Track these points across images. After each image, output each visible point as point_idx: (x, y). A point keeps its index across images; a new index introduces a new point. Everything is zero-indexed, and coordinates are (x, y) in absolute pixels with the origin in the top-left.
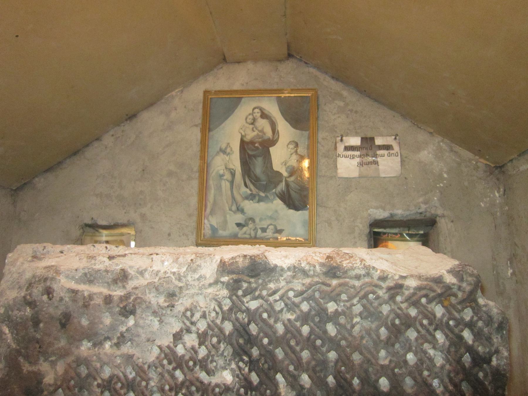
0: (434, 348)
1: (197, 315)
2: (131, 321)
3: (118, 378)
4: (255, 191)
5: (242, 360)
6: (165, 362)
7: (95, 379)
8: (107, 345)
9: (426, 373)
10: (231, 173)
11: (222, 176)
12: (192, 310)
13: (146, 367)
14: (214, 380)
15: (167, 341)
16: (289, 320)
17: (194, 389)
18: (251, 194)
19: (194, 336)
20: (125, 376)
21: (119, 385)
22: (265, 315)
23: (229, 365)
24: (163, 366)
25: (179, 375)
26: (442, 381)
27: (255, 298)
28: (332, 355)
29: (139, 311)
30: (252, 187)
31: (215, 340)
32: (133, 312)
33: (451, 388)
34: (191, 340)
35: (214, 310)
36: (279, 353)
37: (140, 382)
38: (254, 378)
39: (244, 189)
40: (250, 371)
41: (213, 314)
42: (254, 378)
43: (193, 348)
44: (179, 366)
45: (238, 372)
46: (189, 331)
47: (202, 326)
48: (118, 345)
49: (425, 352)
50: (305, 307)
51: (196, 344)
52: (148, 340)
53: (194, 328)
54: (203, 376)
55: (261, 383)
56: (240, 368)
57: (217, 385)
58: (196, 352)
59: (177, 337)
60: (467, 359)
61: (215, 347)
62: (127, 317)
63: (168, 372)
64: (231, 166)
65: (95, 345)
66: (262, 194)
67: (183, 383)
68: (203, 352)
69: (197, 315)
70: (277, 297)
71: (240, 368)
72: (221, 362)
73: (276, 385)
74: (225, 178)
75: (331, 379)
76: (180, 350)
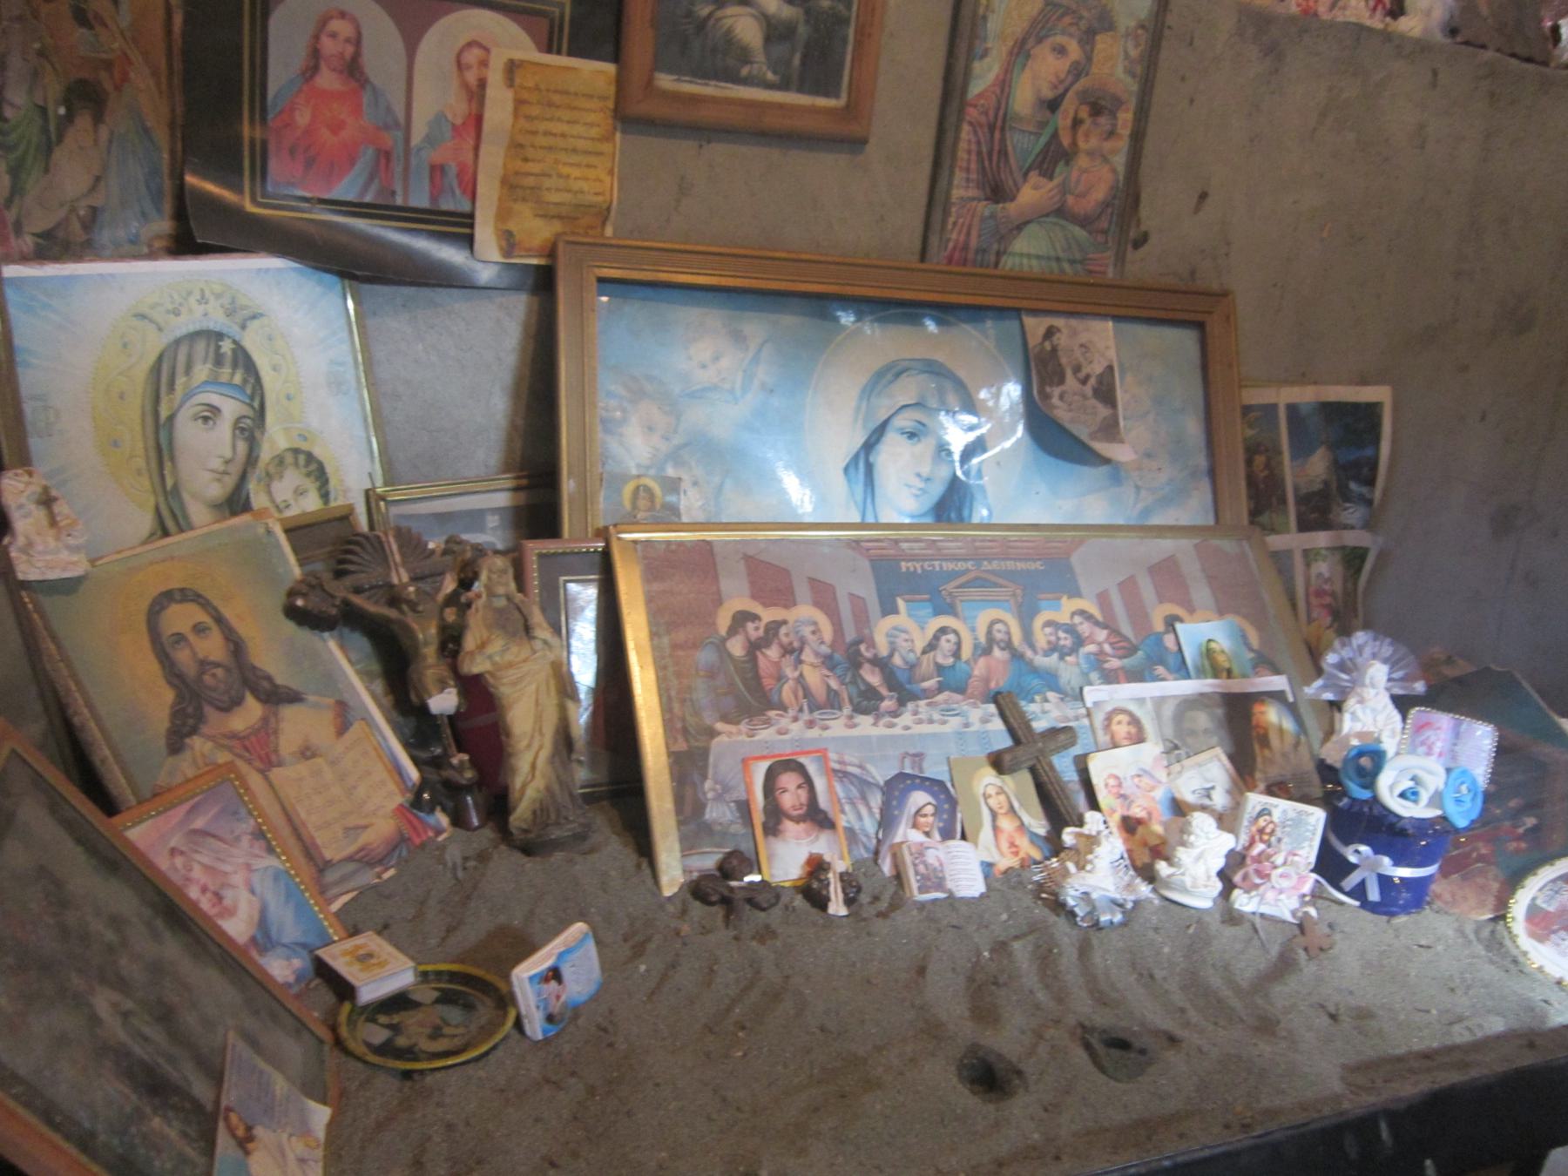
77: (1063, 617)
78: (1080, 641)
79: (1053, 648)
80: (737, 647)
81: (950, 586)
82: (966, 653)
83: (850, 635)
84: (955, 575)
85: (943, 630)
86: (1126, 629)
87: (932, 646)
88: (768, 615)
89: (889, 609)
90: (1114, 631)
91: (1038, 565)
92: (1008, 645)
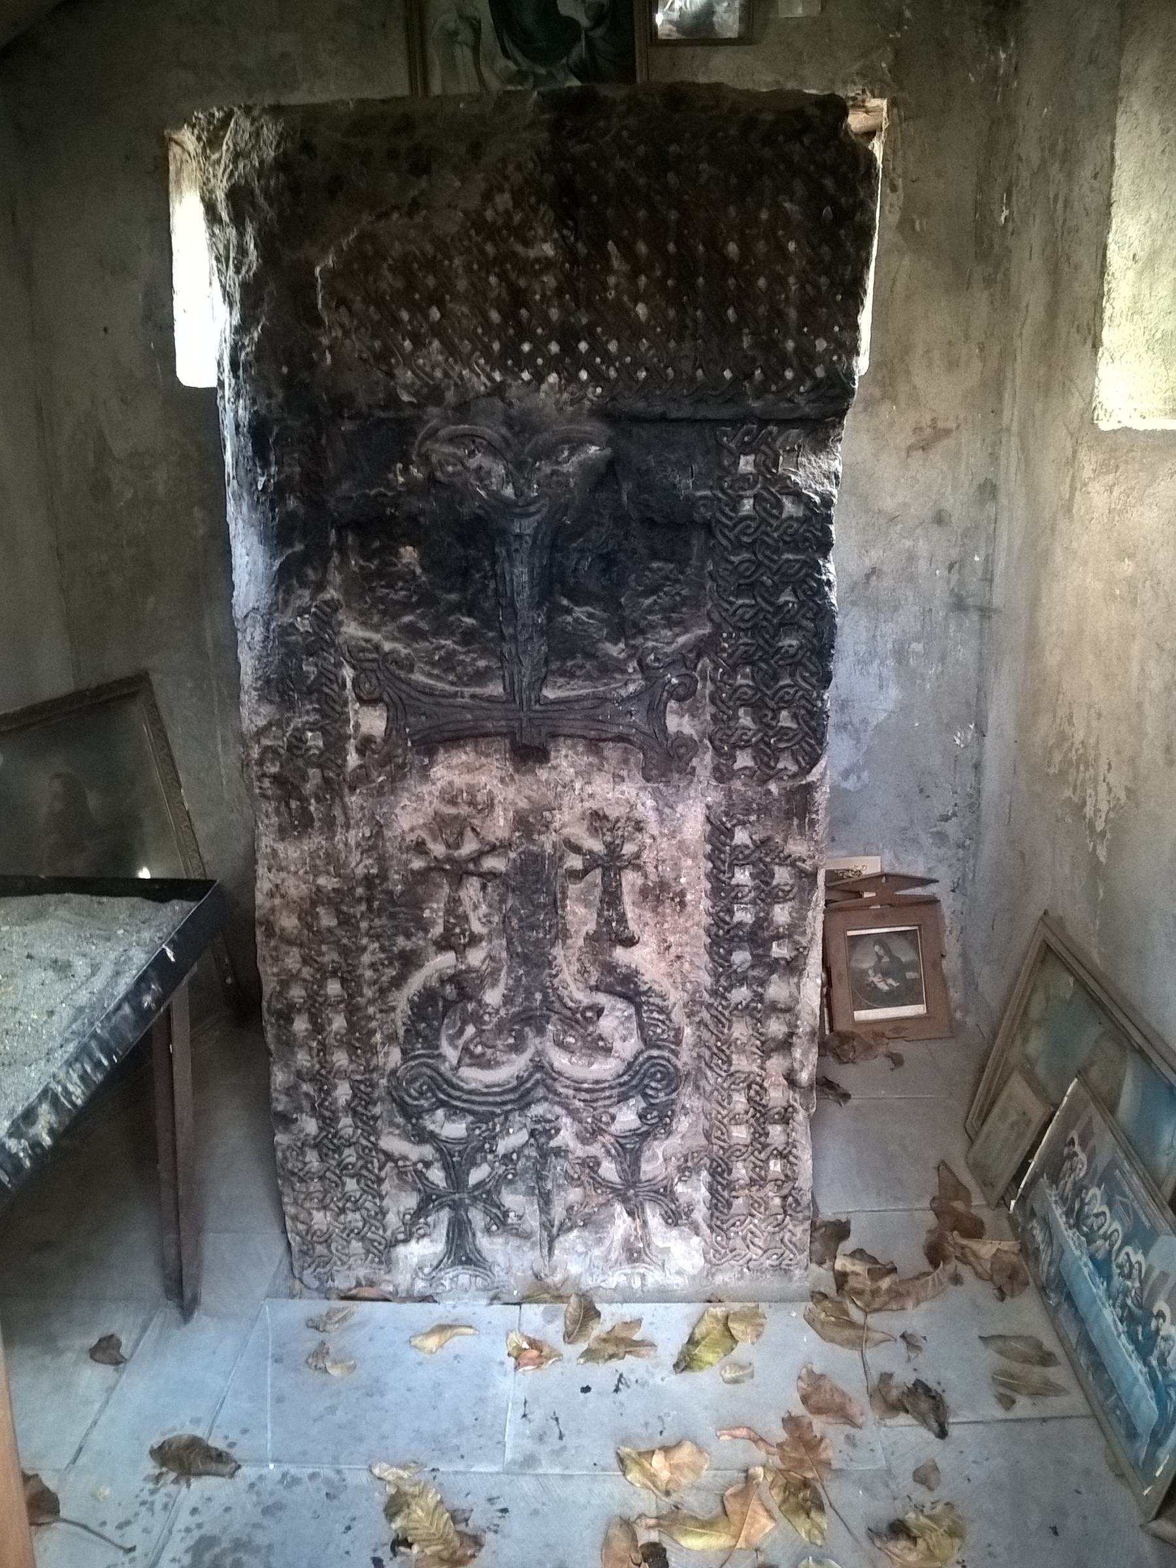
0: (791, 201)
1: (511, 167)
2: (424, 183)
3: (415, 256)
4: (525, 64)
5: (567, 227)
6: (473, 232)
7: (385, 259)
8: (395, 216)
9: (781, 233)
10: (471, 24)
11: (455, 33)
12: (504, 160)
13: (448, 240)
14: (532, 254)
15: (474, 203)
16: (623, 170)
17: (509, 266)
18: (519, 72)
19: (507, 196)
20: (423, 254)
21: (416, 266)
22: (594, 164)
23: (551, 233)
24: (470, 238)
25: (490, 249)
26: (798, 243)
27: (583, 142)
28: (673, 215)
29: (434, 166)
30: (519, 56)
31: (533, 200)
32: (427, 170)
33: (808, 250)
34: (503, 200)
35: (532, 159)
36: (610, 213)
37: (441, 262)
38: (582, 249)
39: (502, 63)
40: (576, 239)
41: (531, 165)
42: (582, 249)
43: (507, 212)
44: (490, 238)
45: (561, 242)
46: (501, 190)
47: (517, 178)
48: (410, 214)
49: (779, 206)
50: (641, 150)
51: (510, 205)
52: (449, 206)
53: (507, 186)
54: (519, 249)
55: (589, 254)
56: (563, 237)
57: (537, 260)
58: (510, 218)
59: (487, 197)
60: (827, 211)
61: (535, 210)
62: (418, 176)
63: (477, 244)
64: (470, 11)
65: (379, 217)
66: (542, 71)
67: (495, 258)
68: (517, 218)
69: (511, 167)
70: (608, 138)
71: (563, 237)
72: (541, 232)
73: (606, 257)
74: (460, 38)
75: (671, 247)
76: (489, 214)
77: (1133, 1260)
78: (1129, 1276)
79: (1120, 1267)
80: (1066, 1151)
81: (1118, 1198)
82: (1101, 1232)
83: (1085, 1183)
84: (1125, 1196)
85: (1104, 1213)
86: (1146, 1294)
87: (1097, 1215)
88: (1077, 1148)
89: (1099, 1187)
90: (1142, 1289)
91: (1147, 1224)
92: (1112, 1246)
